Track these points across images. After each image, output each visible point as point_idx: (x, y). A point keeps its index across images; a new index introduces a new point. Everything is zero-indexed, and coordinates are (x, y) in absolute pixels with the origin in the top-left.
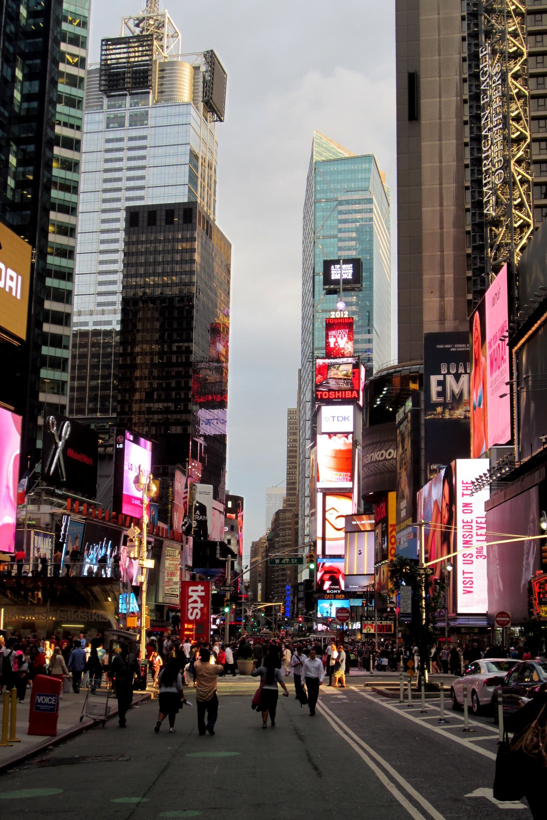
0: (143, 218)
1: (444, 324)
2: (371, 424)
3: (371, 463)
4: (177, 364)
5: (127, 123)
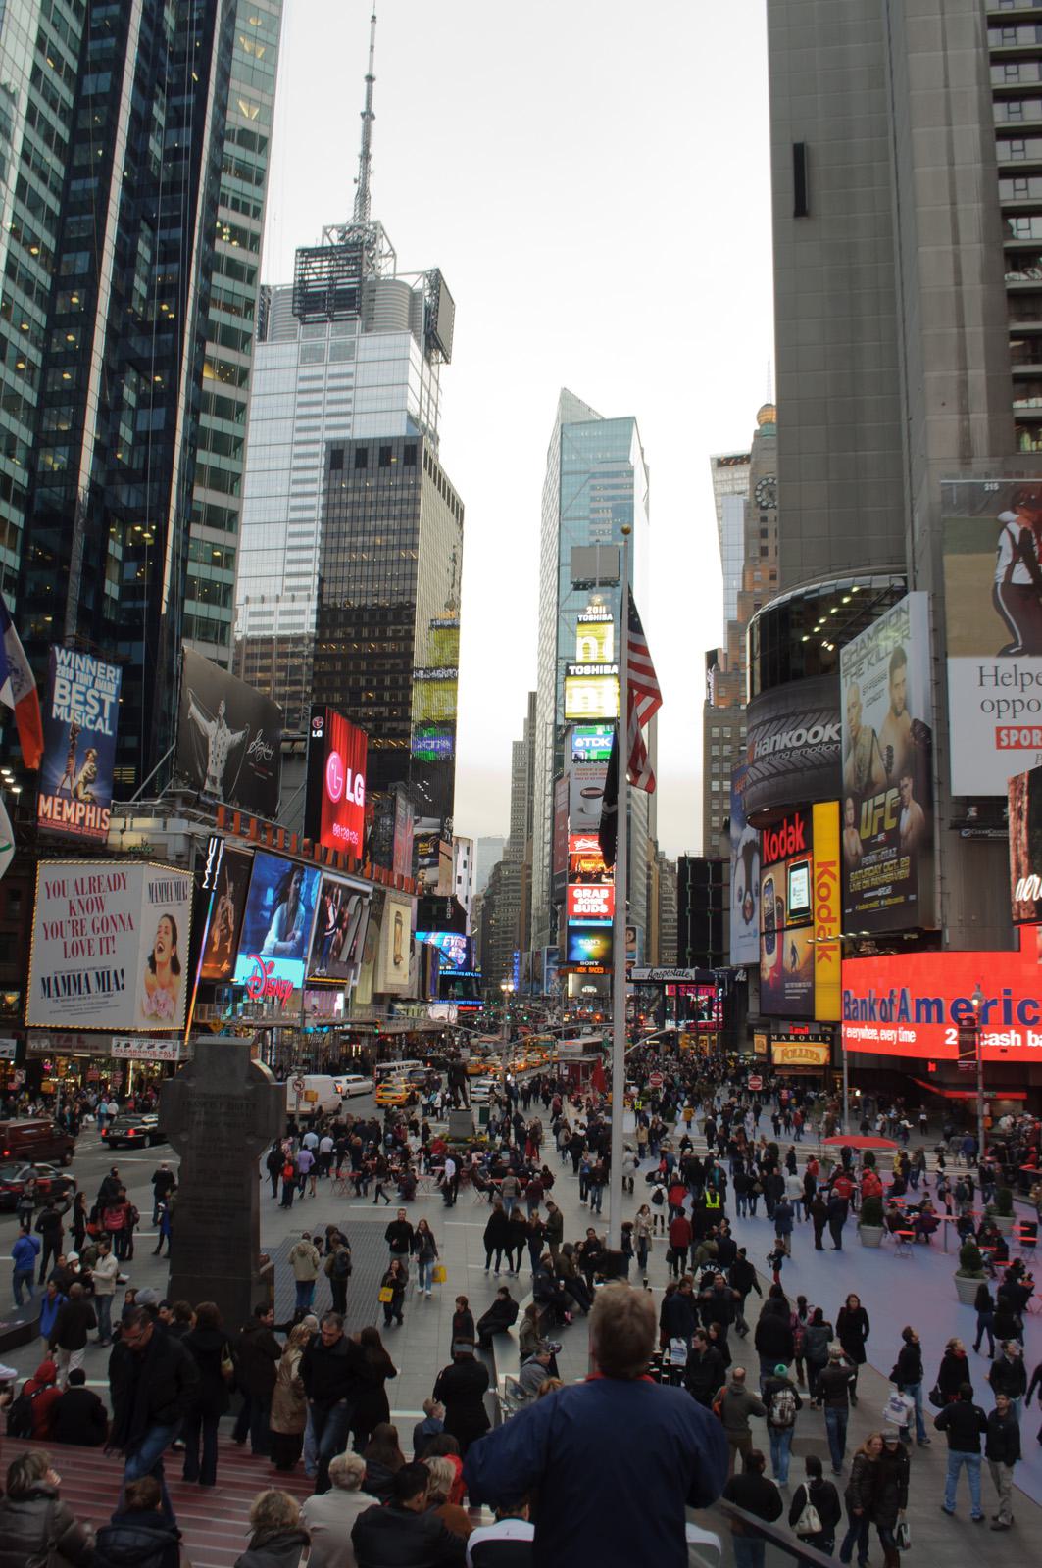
0: (349, 459)
1: (969, 463)
2: (763, 687)
3: (774, 753)
4: (394, 655)
5: (327, 357)
